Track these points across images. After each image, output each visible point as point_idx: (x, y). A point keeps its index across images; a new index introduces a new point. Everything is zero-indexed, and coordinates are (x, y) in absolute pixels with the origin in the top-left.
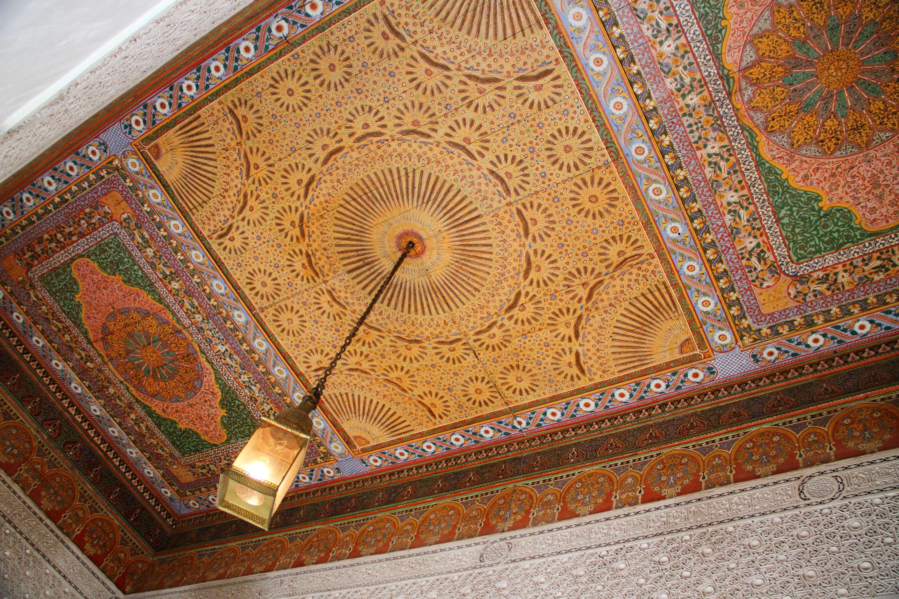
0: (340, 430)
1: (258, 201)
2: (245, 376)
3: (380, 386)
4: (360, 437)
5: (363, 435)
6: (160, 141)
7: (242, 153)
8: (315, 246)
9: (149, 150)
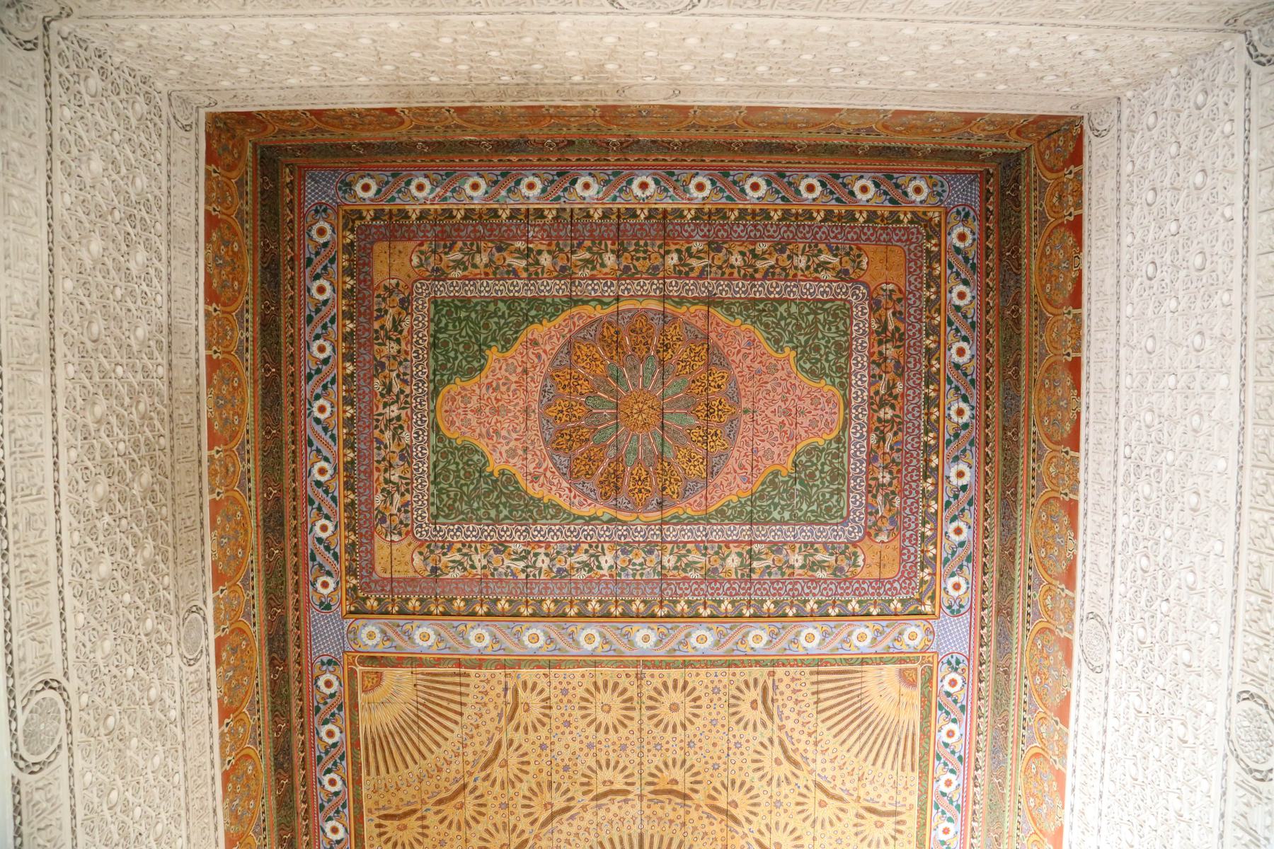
0: (399, 662)
1: (783, 778)
2: (545, 566)
3: (457, 771)
4: (379, 684)
5: (379, 691)
6: (916, 693)
7: (846, 797)
8: (694, 815)
9: (916, 669)
